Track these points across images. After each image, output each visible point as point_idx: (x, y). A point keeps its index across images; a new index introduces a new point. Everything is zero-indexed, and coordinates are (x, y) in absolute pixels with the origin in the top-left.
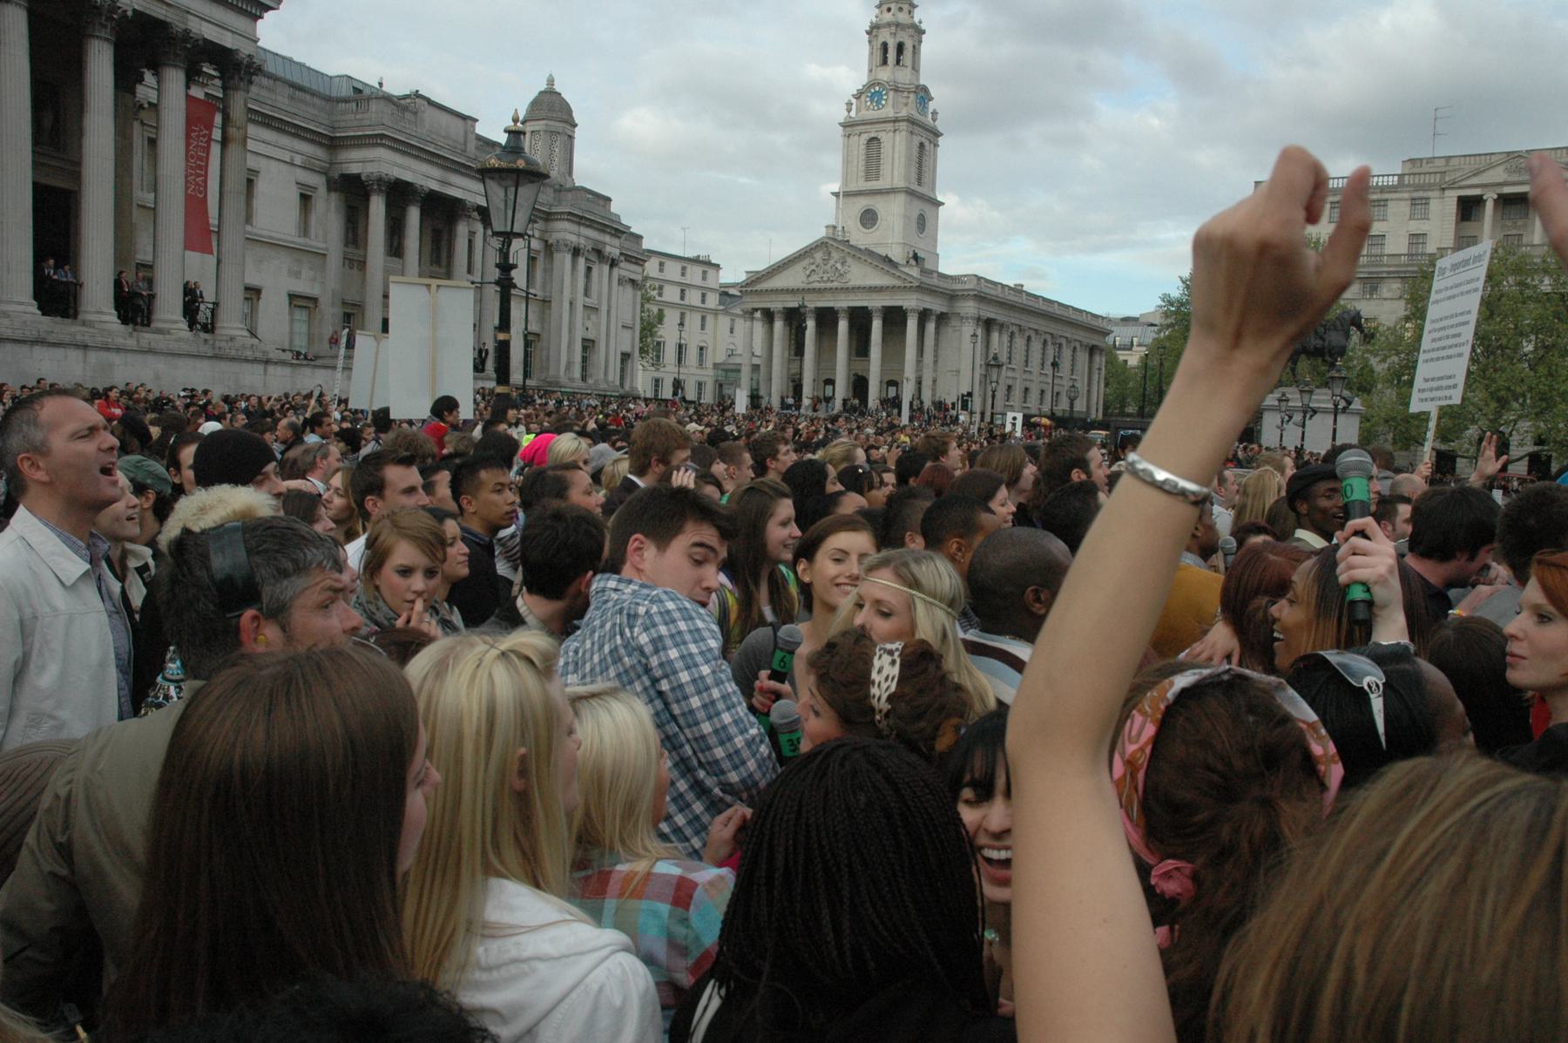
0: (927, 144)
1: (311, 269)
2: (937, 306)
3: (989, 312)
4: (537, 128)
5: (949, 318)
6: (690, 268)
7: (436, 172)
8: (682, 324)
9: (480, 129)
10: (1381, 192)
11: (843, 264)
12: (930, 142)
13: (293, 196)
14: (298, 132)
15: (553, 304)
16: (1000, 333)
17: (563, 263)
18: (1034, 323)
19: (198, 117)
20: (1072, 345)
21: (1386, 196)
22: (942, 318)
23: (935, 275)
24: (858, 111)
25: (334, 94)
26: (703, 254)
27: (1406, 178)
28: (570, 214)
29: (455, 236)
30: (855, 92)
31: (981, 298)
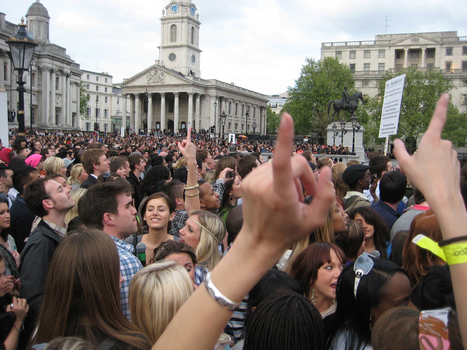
0: (195, 27)
2: (200, 92)
3: (221, 94)
5: (205, 97)
8: (97, 101)
11: (162, 75)
16: (226, 102)
18: (239, 98)
20: (254, 106)
21: (370, 49)
22: (202, 97)
23: (199, 80)
24: (167, 14)
26: (105, 72)
27: (377, 42)
28: (48, 55)
30: (166, 6)
31: (218, 88)
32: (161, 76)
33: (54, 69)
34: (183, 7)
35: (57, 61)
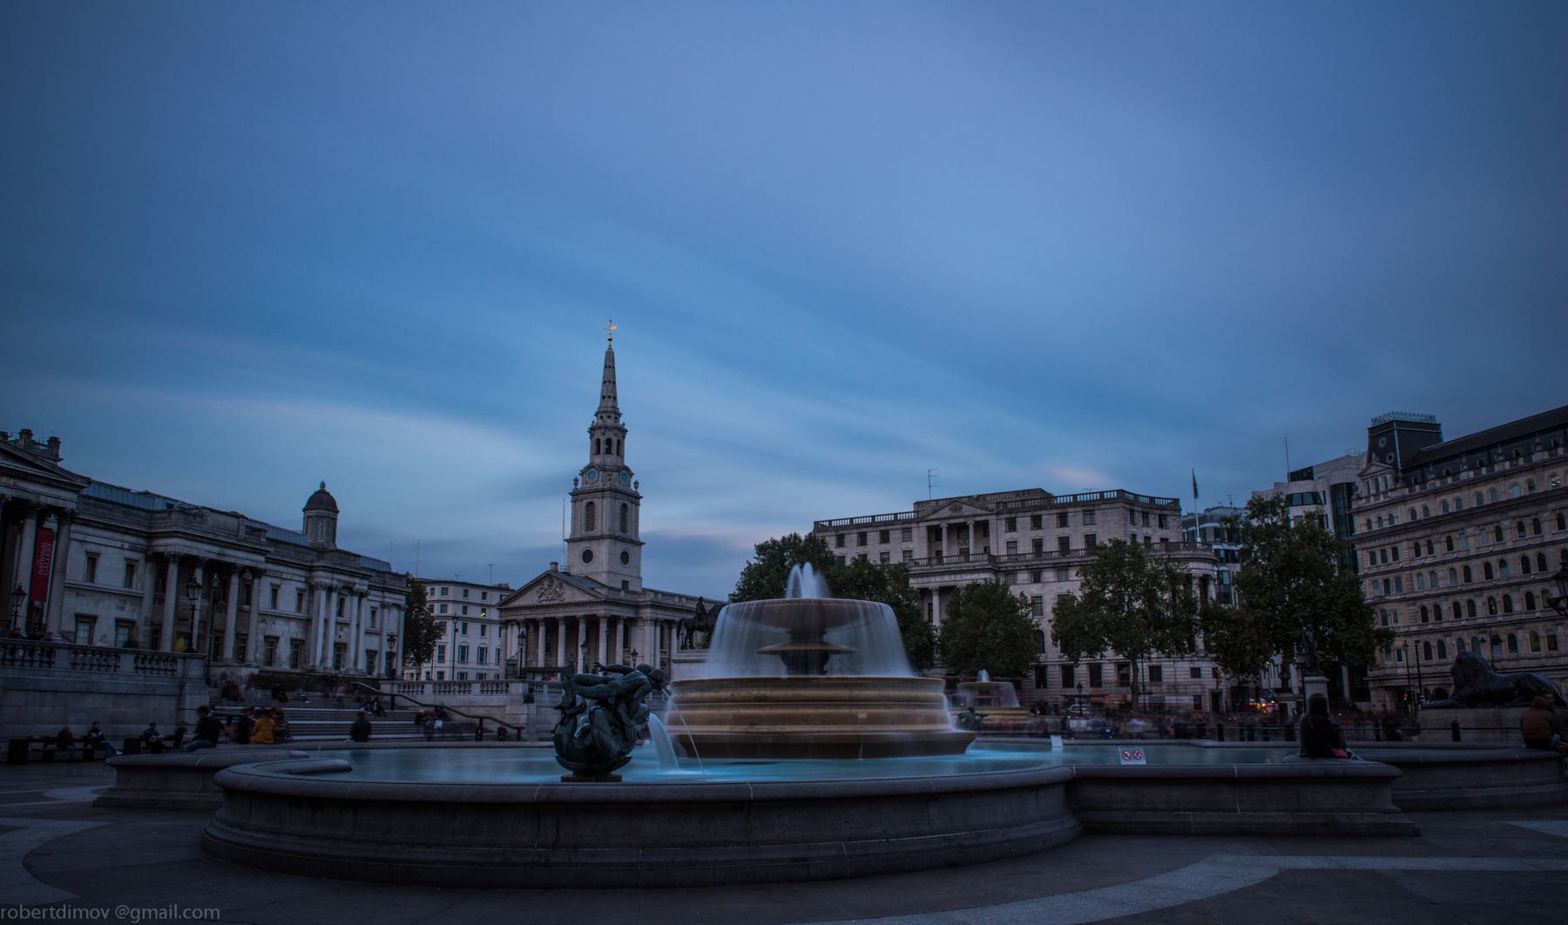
0: (629, 504)
1: (132, 605)
2: (625, 613)
3: (662, 615)
4: (311, 514)
5: (637, 621)
6: (489, 594)
7: (216, 549)
10: (885, 525)
11: (561, 588)
13: (122, 565)
14: (127, 532)
15: (313, 622)
19: (43, 536)
22: (630, 623)
26: (504, 582)
33: (334, 586)
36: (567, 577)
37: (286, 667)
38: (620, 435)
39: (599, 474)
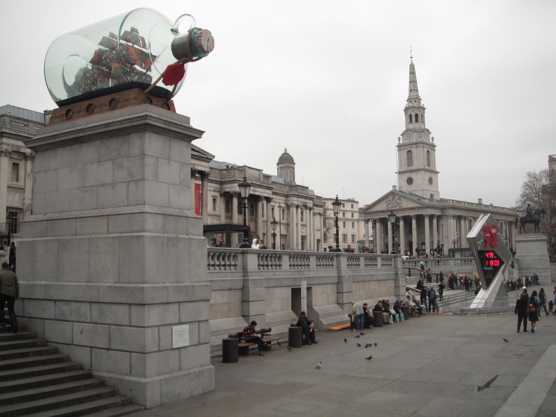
0: (430, 150)
2: (437, 213)
4: (282, 166)
9: (264, 172)
11: (400, 199)
12: (432, 149)
16: (465, 220)
17: (293, 210)
20: (500, 222)
22: (439, 218)
23: (435, 201)
24: (403, 140)
25: (220, 168)
26: (351, 197)
28: (294, 194)
29: (258, 207)
30: (401, 134)
31: (454, 208)
32: (398, 201)
33: (299, 205)
34: (417, 133)
35: (301, 198)
36: (402, 193)
37: (279, 250)
38: (422, 111)
39: (413, 133)
